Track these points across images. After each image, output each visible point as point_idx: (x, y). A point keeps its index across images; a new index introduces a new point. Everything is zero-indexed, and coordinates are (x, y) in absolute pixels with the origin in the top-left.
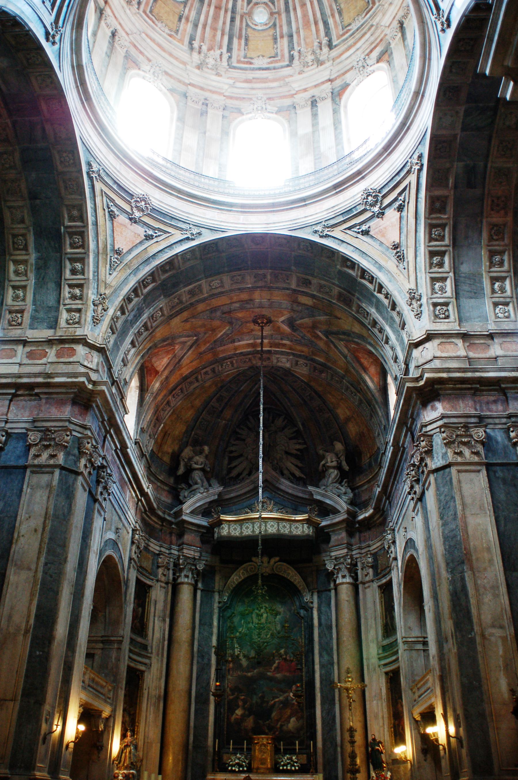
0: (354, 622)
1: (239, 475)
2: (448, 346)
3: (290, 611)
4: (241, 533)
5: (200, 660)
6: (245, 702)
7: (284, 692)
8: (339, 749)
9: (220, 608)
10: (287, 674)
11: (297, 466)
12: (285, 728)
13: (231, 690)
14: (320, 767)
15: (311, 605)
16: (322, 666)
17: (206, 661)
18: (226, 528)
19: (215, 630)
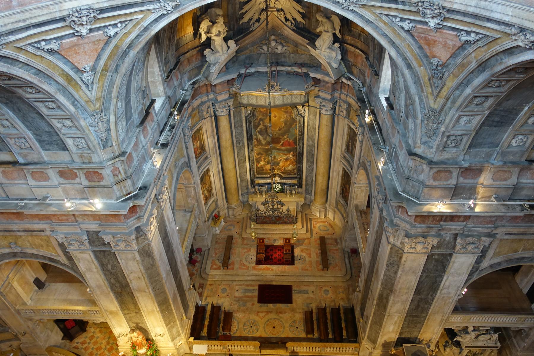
0: (329, 137)
1: (251, 19)
2: (443, 175)
3: (290, 116)
4: (257, 102)
5: (238, 145)
6: (265, 159)
7: (286, 155)
8: (314, 182)
9: (246, 117)
10: (288, 147)
11: (298, 11)
12: (286, 169)
13: (257, 154)
14: (304, 186)
15: (303, 115)
16: (308, 146)
17: (241, 144)
18: (246, 99)
19: (245, 129)
